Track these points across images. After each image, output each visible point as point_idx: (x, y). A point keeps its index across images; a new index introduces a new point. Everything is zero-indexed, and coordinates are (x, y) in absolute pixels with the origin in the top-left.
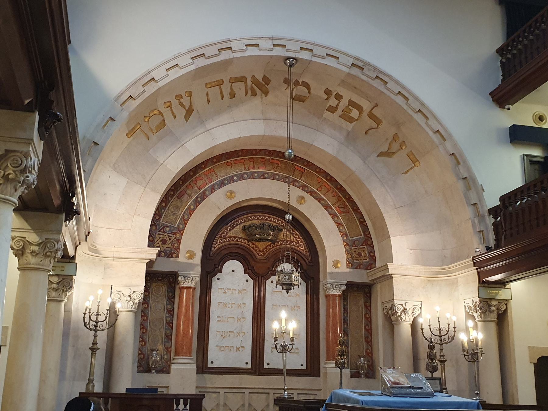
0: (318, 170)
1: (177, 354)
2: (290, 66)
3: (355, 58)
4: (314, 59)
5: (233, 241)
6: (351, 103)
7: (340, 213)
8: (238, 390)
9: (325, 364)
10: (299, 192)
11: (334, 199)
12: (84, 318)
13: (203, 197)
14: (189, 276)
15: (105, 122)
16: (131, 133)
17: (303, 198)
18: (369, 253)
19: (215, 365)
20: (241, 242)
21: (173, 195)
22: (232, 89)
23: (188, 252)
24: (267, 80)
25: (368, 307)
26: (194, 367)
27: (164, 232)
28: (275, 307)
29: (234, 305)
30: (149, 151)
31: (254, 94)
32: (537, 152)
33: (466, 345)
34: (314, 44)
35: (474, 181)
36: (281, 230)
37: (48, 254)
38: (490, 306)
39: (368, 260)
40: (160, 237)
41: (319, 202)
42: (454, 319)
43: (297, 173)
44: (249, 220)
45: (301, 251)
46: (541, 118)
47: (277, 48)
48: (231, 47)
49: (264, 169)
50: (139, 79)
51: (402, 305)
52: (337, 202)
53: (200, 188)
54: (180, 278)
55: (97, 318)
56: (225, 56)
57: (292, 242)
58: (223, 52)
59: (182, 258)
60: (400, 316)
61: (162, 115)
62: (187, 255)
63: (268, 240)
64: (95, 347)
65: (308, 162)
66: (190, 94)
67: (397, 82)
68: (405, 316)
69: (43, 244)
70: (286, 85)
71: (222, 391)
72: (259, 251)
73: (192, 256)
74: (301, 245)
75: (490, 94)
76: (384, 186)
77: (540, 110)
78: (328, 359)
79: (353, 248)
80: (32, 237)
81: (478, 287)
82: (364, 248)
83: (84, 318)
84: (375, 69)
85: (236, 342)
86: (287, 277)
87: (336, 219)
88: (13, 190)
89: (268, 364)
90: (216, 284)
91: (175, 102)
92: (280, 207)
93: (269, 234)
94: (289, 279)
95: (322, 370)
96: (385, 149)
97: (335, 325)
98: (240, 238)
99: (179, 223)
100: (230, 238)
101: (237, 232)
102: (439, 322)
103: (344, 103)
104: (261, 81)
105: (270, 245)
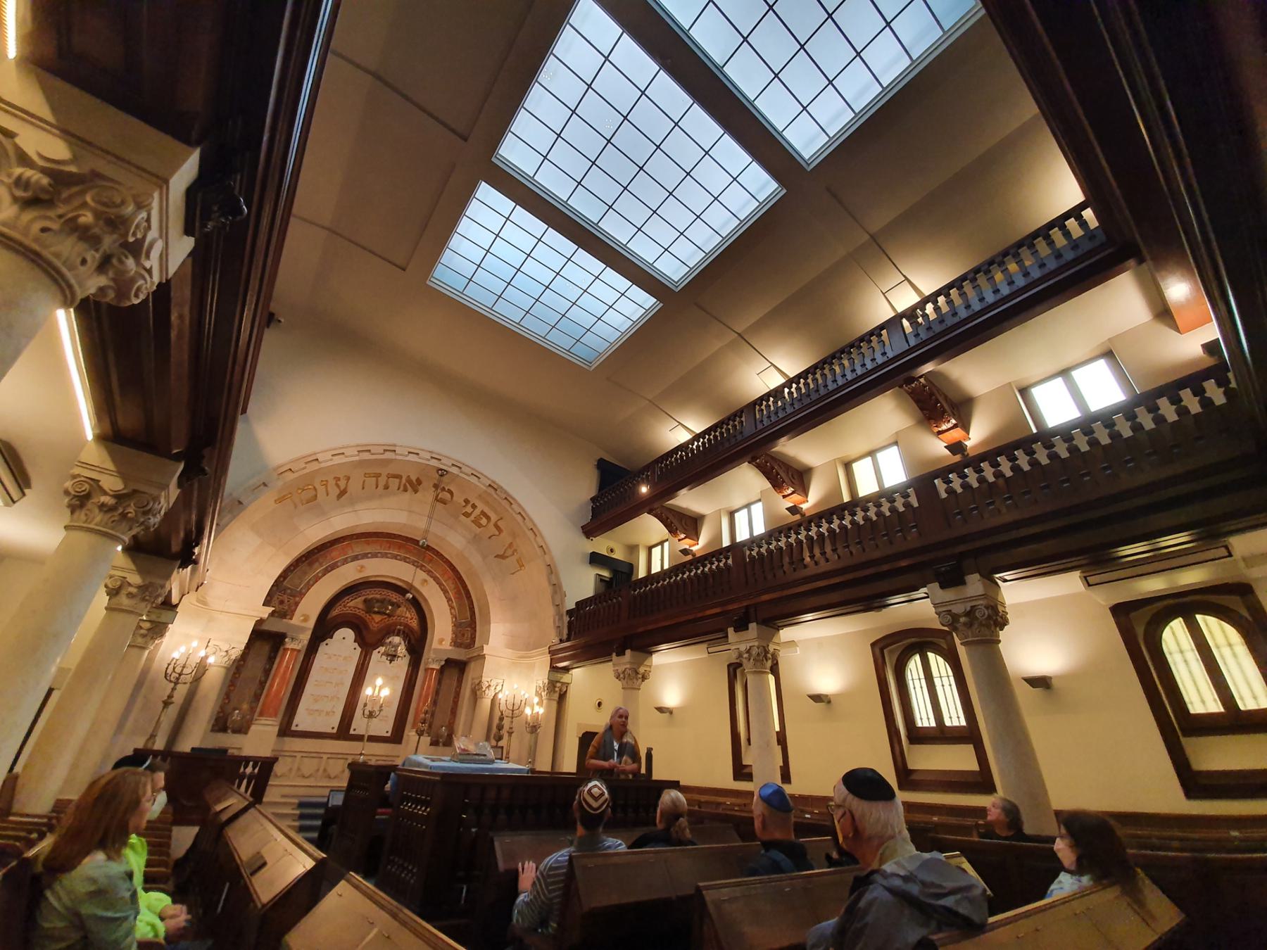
1: (261, 714)
2: (441, 476)
3: (494, 482)
4: (461, 475)
6: (483, 513)
8: (318, 755)
9: (409, 732)
10: (424, 575)
11: (453, 586)
12: (167, 669)
16: (280, 500)
17: (425, 581)
19: (299, 729)
23: (303, 615)
24: (419, 482)
25: (460, 681)
26: (276, 729)
31: (405, 490)
32: (606, 574)
33: (529, 718)
36: (399, 607)
37: (147, 598)
38: (555, 687)
40: (278, 598)
42: (526, 696)
43: (426, 559)
44: (373, 594)
47: (434, 460)
50: (304, 457)
53: (333, 559)
54: (287, 640)
55: (182, 670)
56: (389, 455)
57: (407, 618)
58: (387, 453)
59: (296, 620)
62: (302, 618)
63: (386, 614)
64: (170, 701)
65: (438, 552)
66: (348, 479)
67: (520, 505)
69: (143, 588)
70: (434, 489)
71: (299, 755)
72: (375, 622)
73: (306, 619)
77: (612, 544)
78: (413, 727)
80: (135, 579)
81: (549, 671)
83: (167, 669)
84: (506, 492)
86: (393, 649)
87: (450, 602)
88: (127, 527)
90: (323, 648)
91: (332, 482)
93: (387, 609)
94: (394, 651)
95: (405, 737)
100: (350, 607)
101: (357, 602)
103: (477, 512)
104: (414, 481)
105: (385, 618)
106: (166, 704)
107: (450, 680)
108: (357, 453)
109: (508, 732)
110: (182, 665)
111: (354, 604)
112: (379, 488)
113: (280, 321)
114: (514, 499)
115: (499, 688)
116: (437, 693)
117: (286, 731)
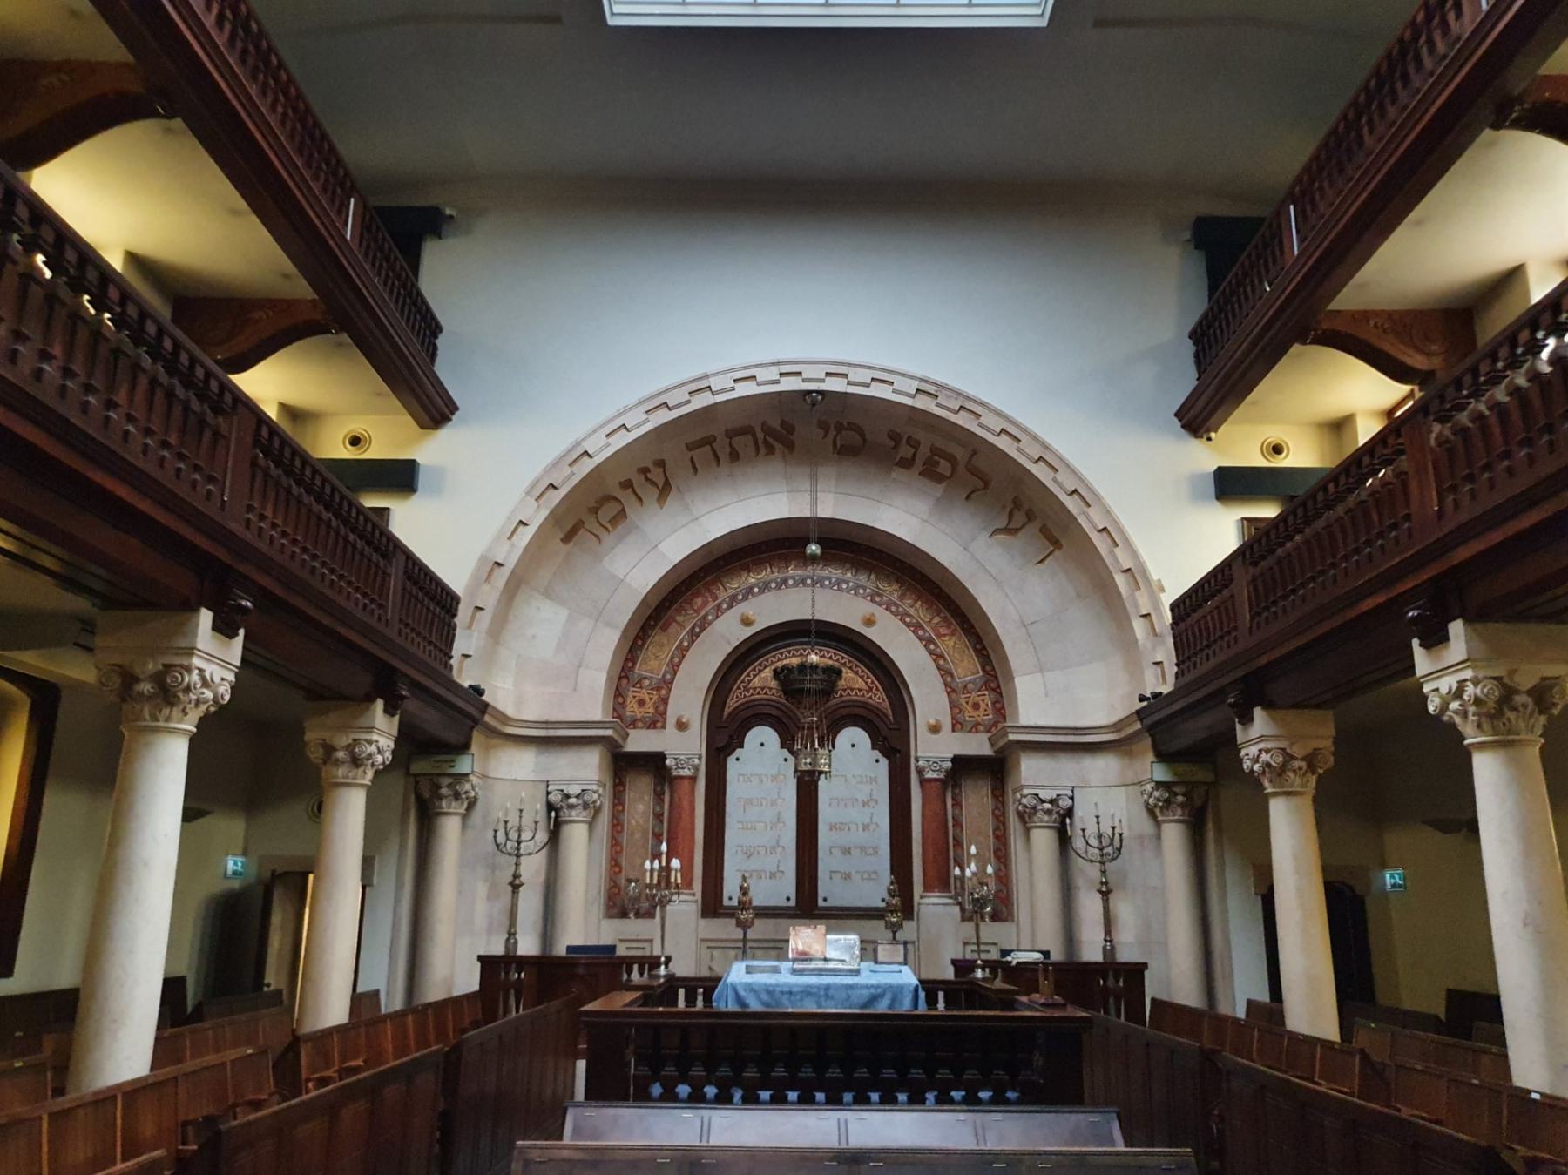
5: (759, 693)
6: (935, 451)
9: (922, 897)
12: (495, 837)
13: (703, 625)
18: (994, 704)
21: (655, 626)
27: (641, 688)
34: (850, 365)
35: (1144, 573)
36: (839, 672)
39: (991, 716)
40: (634, 697)
46: (1277, 449)
48: (709, 387)
50: (564, 456)
53: (697, 611)
55: (519, 836)
57: (860, 690)
64: (517, 882)
66: (661, 464)
74: (875, 695)
75: (1176, 415)
77: (1274, 434)
83: (495, 837)
85: (770, 863)
89: (825, 900)
91: (638, 480)
100: (755, 689)
103: (924, 451)
104: (779, 428)
106: (515, 887)
107: (976, 800)
108: (645, 417)
109: (1100, 891)
110: (516, 828)
111: (762, 680)
114: (983, 404)
117: (712, 906)
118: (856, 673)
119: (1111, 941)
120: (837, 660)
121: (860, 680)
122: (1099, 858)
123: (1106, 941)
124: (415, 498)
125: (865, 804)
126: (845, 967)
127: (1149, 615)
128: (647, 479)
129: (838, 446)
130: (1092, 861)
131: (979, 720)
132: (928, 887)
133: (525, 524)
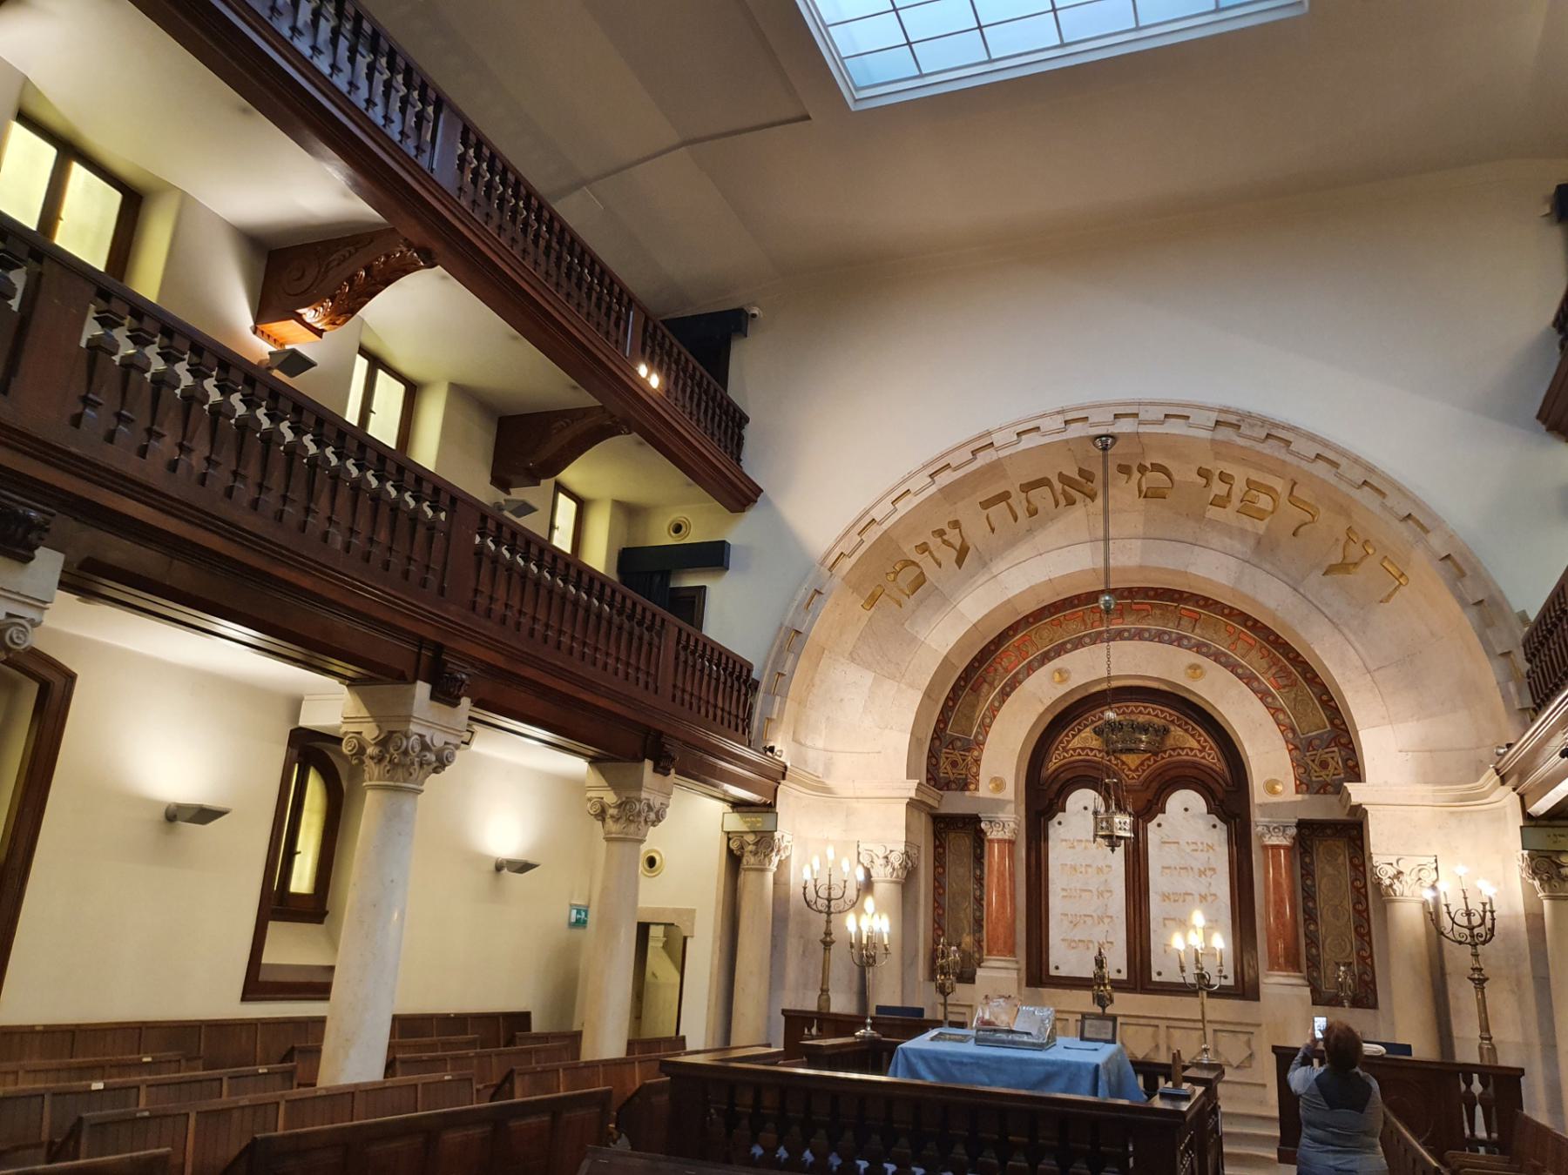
0: (1226, 611)
1: (989, 953)
4: (1142, 429)
5: (1080, 755)
7: (1278, 689)
9: (1267, 976)
10: (1192, 657)
11: (1264, 663)
12: (804, 894)
14: (997, 820)
15: (809, 597)
17: (1194, 667)
18: (1345, 761)
19: (1063, 972)
20: (1095, 756)
21: (965, 687)
22: (1028, 501)
23: (994, 780)
27: (953, 749)
28: (1167, 871)
29: (1089, 870)
30: (903, 624)
31: (1071, 502)
34: (1140, 404)
36: (1166, 731)
41: (1232, 672)
45: (1210, 765)
47: (1073, 425)
49: (1122, 624)
51: (1391, 864)
52: (1270, 668)
53: (1007, 671)
54: (983, 825)
55: (829, 894)
56: (984, 458)
57: (1192, 749)
58: (980, 455)
59: (985, 790)
60: (1391, 886)
61: (919, 567)
62: (990, 786)
66: (956, 524)
67: (1312, 438)
68: (1401, 887)
70: (1126, 476)
72: (1130, 769)
73: (999, 784)
74: (1209, 755)
76: (1340, 631)
78: (1271, 968)
79: (1308, 754)
80: (610, 798)
81: (1521, 827)
82: (1334, 752)
84: (1264, 421)
85: (1098, 934)
88: (407, 775)
89: (1159, 974)
91: (934, 543)
92: (1164, 687)
96: (1336, 558)
97: (1279, 903)
98: (1092, 750)
99: (977, 733)
100: (1074, 750)
101: (1086, 739)
102: (1465, 898)
103: (1239, 487)
104: (1078, 477)
105: (1149, 759)
111: (1082, 741)
112: (1019, 520)
113: (754, 316)
114: (1293, 429)
115: (1428, 877)
116: (1309, 895)
117: (1038, 975)
118: (1186, 731)
119: (1490, 1039)
120: (1165, 718)
121: (1191, 739)
122: (1469, 940)
123: (1482, 1038)
124: (729, 572)
125: (1202, 873)
126: (1031, 1040)
127: (1509, 652)
128: (944, 542)
129: (1144, 488)
130: (1460, 943)
131: (1328, 780)
132: (1274, 965)
133: (819, 593)
